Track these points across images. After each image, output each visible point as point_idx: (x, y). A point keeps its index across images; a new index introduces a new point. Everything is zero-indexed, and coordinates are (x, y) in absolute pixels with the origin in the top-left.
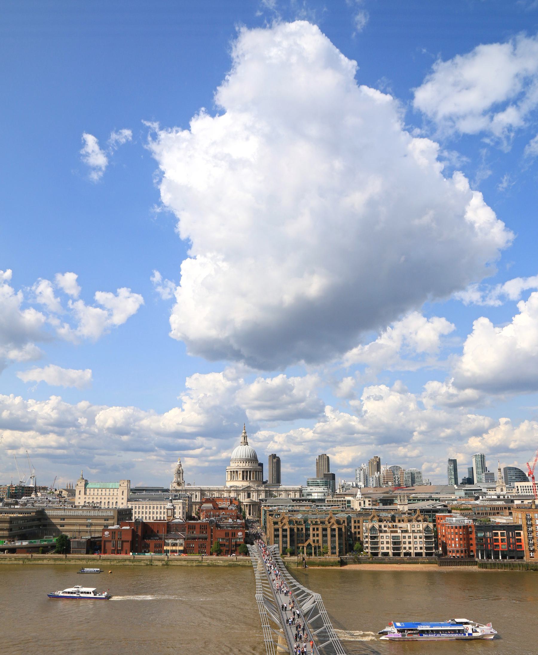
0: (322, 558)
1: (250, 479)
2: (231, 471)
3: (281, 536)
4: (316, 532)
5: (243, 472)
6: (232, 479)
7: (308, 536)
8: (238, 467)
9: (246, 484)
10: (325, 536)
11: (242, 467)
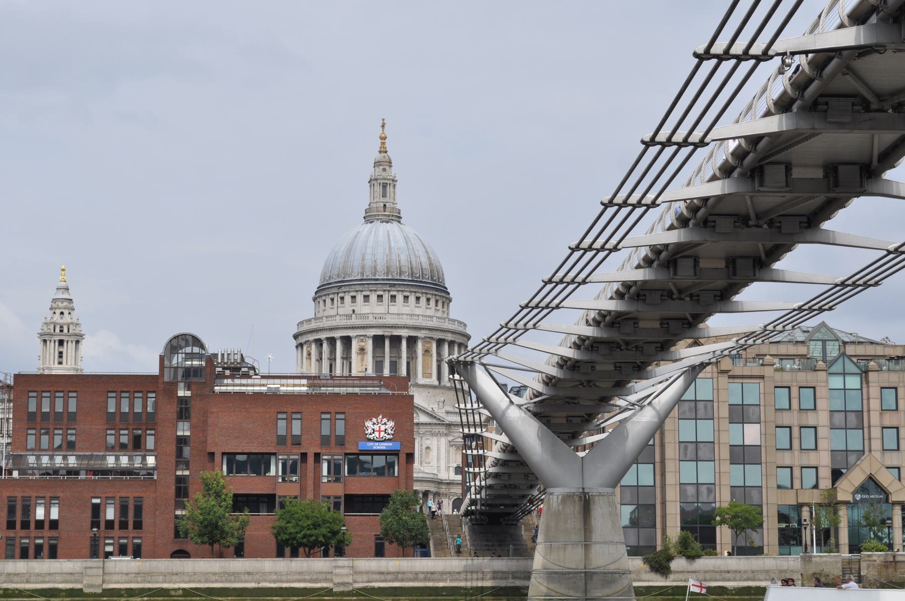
2: (319, 342)
5: (378, 341)
8: (354, 321)
11: (371, 321)
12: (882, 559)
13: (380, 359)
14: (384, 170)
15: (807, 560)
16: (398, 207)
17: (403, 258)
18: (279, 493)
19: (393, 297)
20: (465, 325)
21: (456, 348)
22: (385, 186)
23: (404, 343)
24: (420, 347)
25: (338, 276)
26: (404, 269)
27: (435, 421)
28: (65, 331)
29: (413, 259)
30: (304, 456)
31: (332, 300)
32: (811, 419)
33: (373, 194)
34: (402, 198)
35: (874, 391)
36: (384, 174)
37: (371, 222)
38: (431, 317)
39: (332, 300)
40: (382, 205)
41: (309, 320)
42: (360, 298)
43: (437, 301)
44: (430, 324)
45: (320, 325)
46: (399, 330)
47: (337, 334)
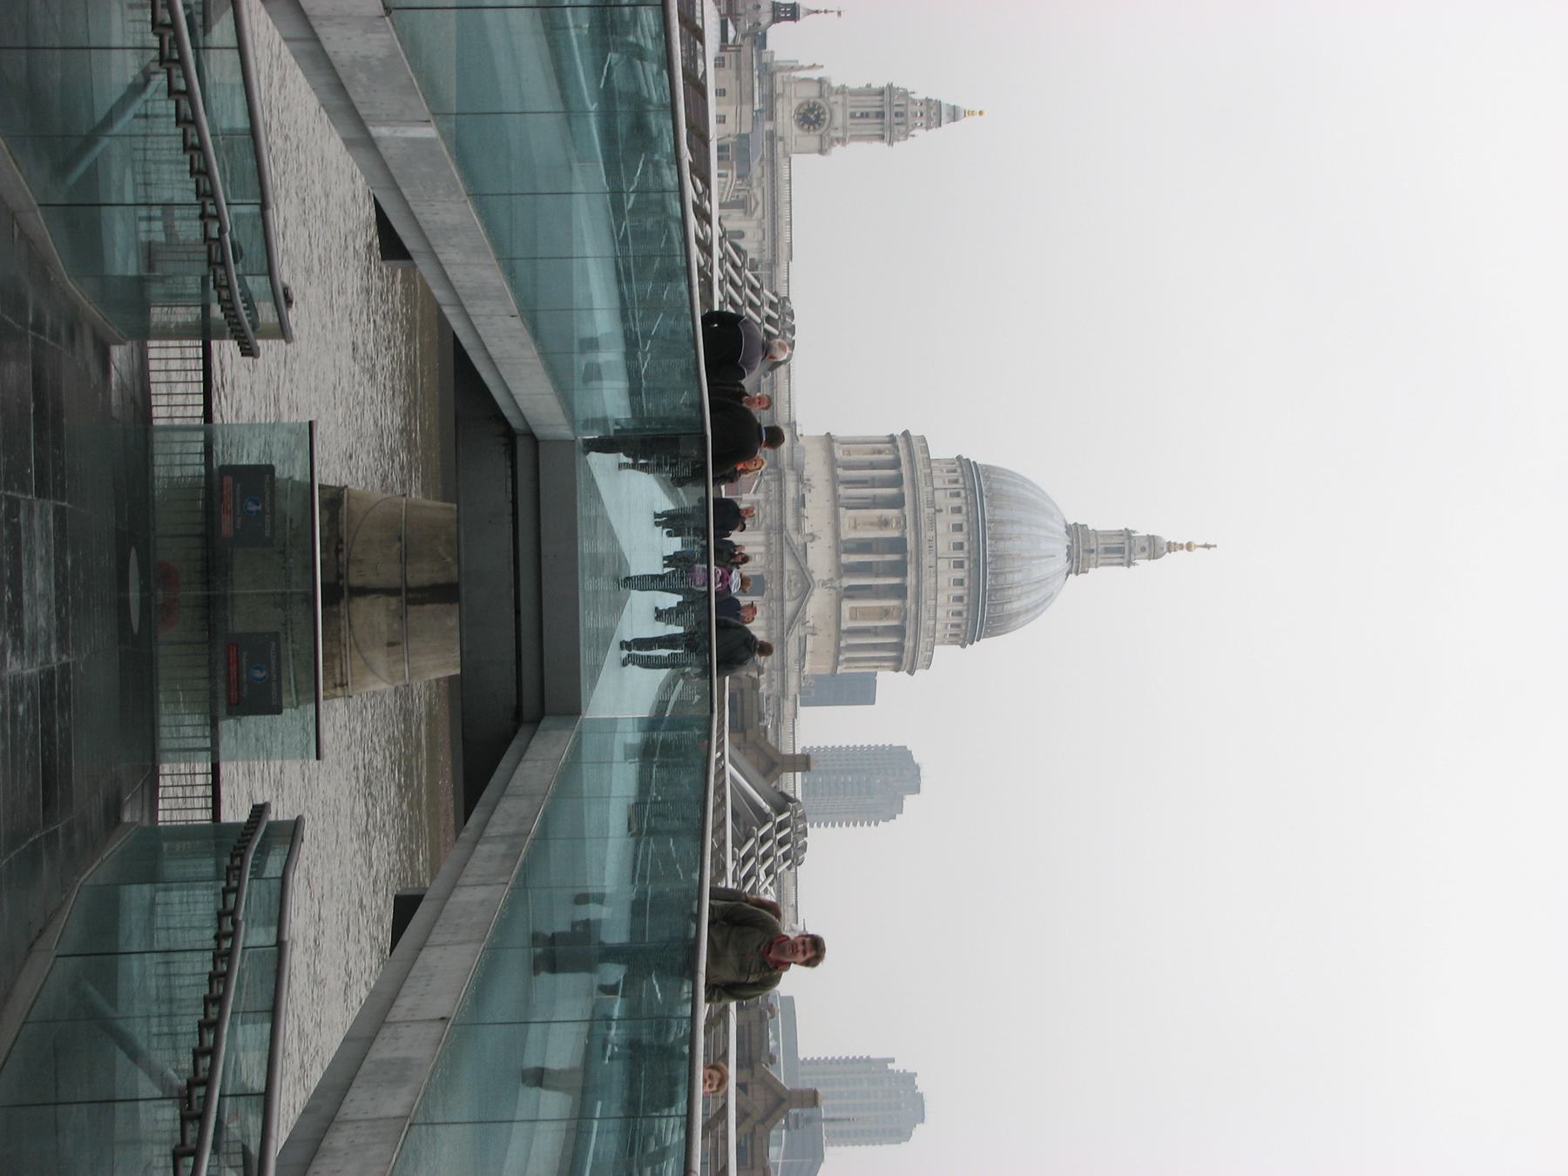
1: (852, 592)
2: (896, 464)
5: (898, 545)
8: (926, 512)
9: (820, 560)
11: (927, 534)
16: (1091, 570)
17: (1017, 577)
19: (959, 565)
20: (928, 667)
22: (1120, 550)
25: (990, 489)
26: (1001, 579)
27: (786, 623)
28: (899, 120)
29: (1017, 591)
31: (956, 481)
33: (1108, 534)
34: (1103, 577)
36: (1137, 549)
38: (935, 618)
39: (956, 481)
42: (958, 519)
43: (958, 626)
44: (924, 615)
45: (920, 466)
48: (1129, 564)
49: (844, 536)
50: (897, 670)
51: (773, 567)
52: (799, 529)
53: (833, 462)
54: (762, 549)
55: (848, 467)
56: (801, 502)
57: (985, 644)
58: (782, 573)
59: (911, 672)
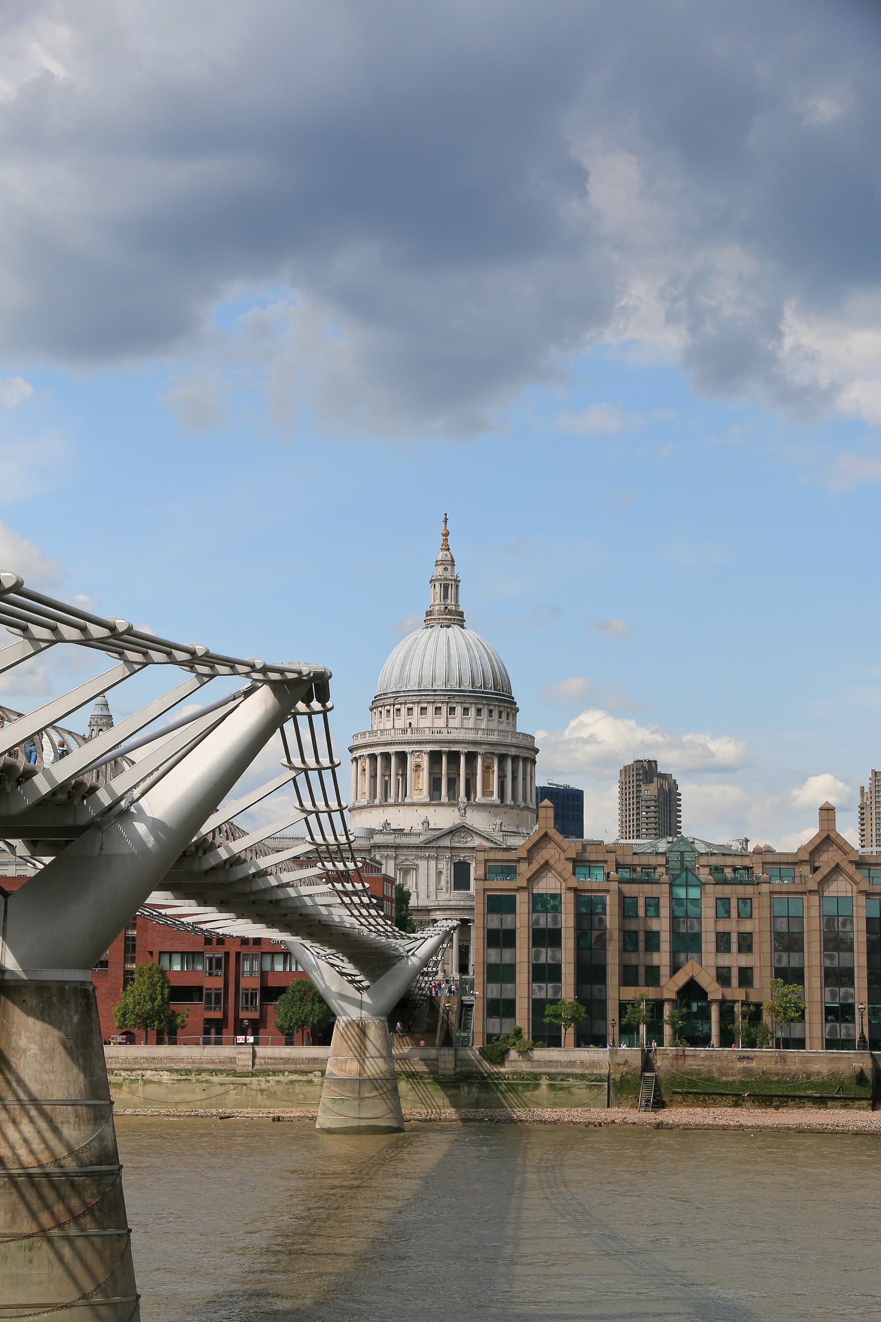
0: (765, 1059)
2: (373, 757)
3: (523, 938)
4: (732, 926)
5: (435, 757)
6: (381, 797)
7: (687, 942)
8: (409, 736)
9: (444, 818)
10: (789, 942)
11: (427, 735)
12: (674, 1053)
13: (438, 776)
14: (446, 569)
15: (613, 1053)
16: (461, 610)
18: (206, 986)
19: (452, 710)
21: (521, 763)
22: (446, 588)
23: (463, 759)
24: (479, 760)
30: (227, 954)
31: (388, 711)
32: (654, 925)
35: (711, 902)
36: (447, 574)
37: (431, 627)
40: (443, 607)
41: (364, 734)
42: (416, 709)
43: (500, 713)
45: (375, 739)
46: (457, 745)
47: (392, 749)
48: (457, 581)
49: (427, 800)
50: (534, 762)
51: (448, 855)
52: (419, 834)
53: (370, 806)
54: (433, 863)
55: (375, 797)
56: (400, 832)
57: (517, 694)
58: (452, 848)
59: (537, 751)
